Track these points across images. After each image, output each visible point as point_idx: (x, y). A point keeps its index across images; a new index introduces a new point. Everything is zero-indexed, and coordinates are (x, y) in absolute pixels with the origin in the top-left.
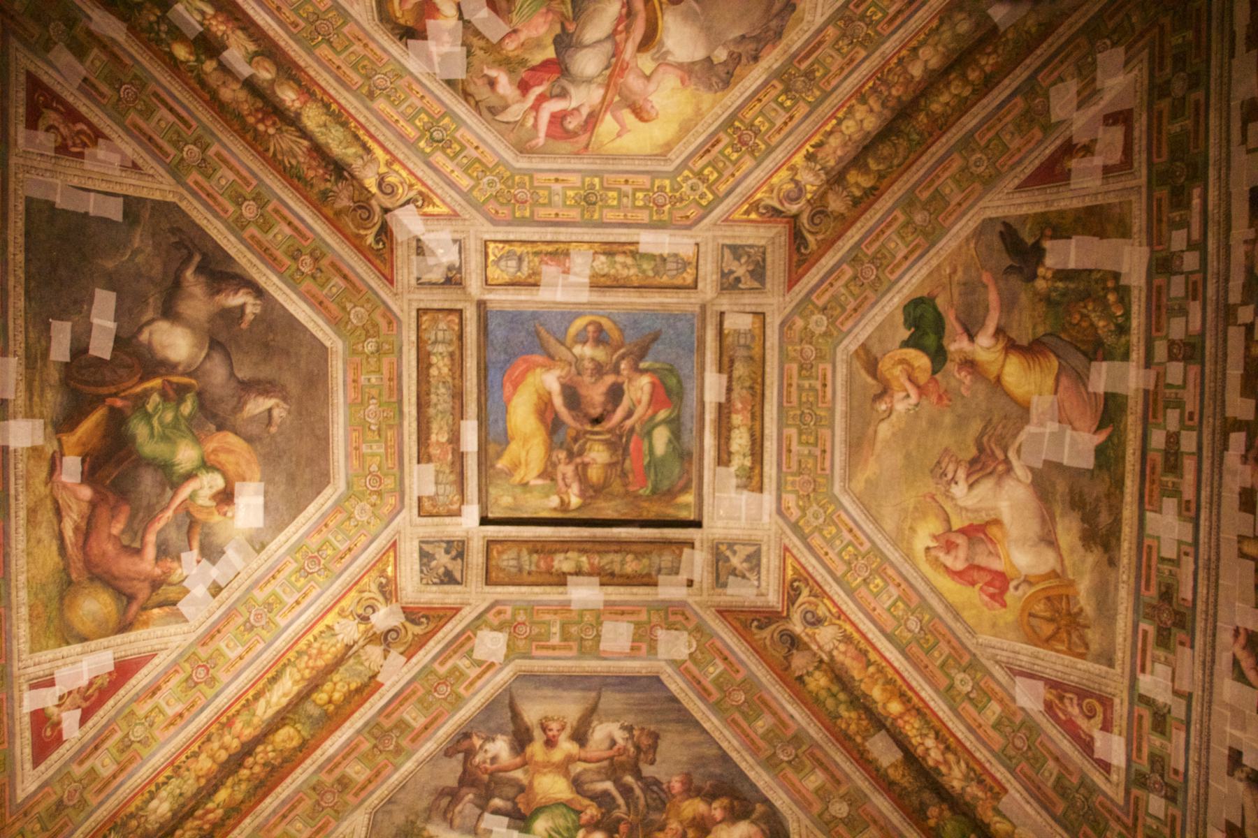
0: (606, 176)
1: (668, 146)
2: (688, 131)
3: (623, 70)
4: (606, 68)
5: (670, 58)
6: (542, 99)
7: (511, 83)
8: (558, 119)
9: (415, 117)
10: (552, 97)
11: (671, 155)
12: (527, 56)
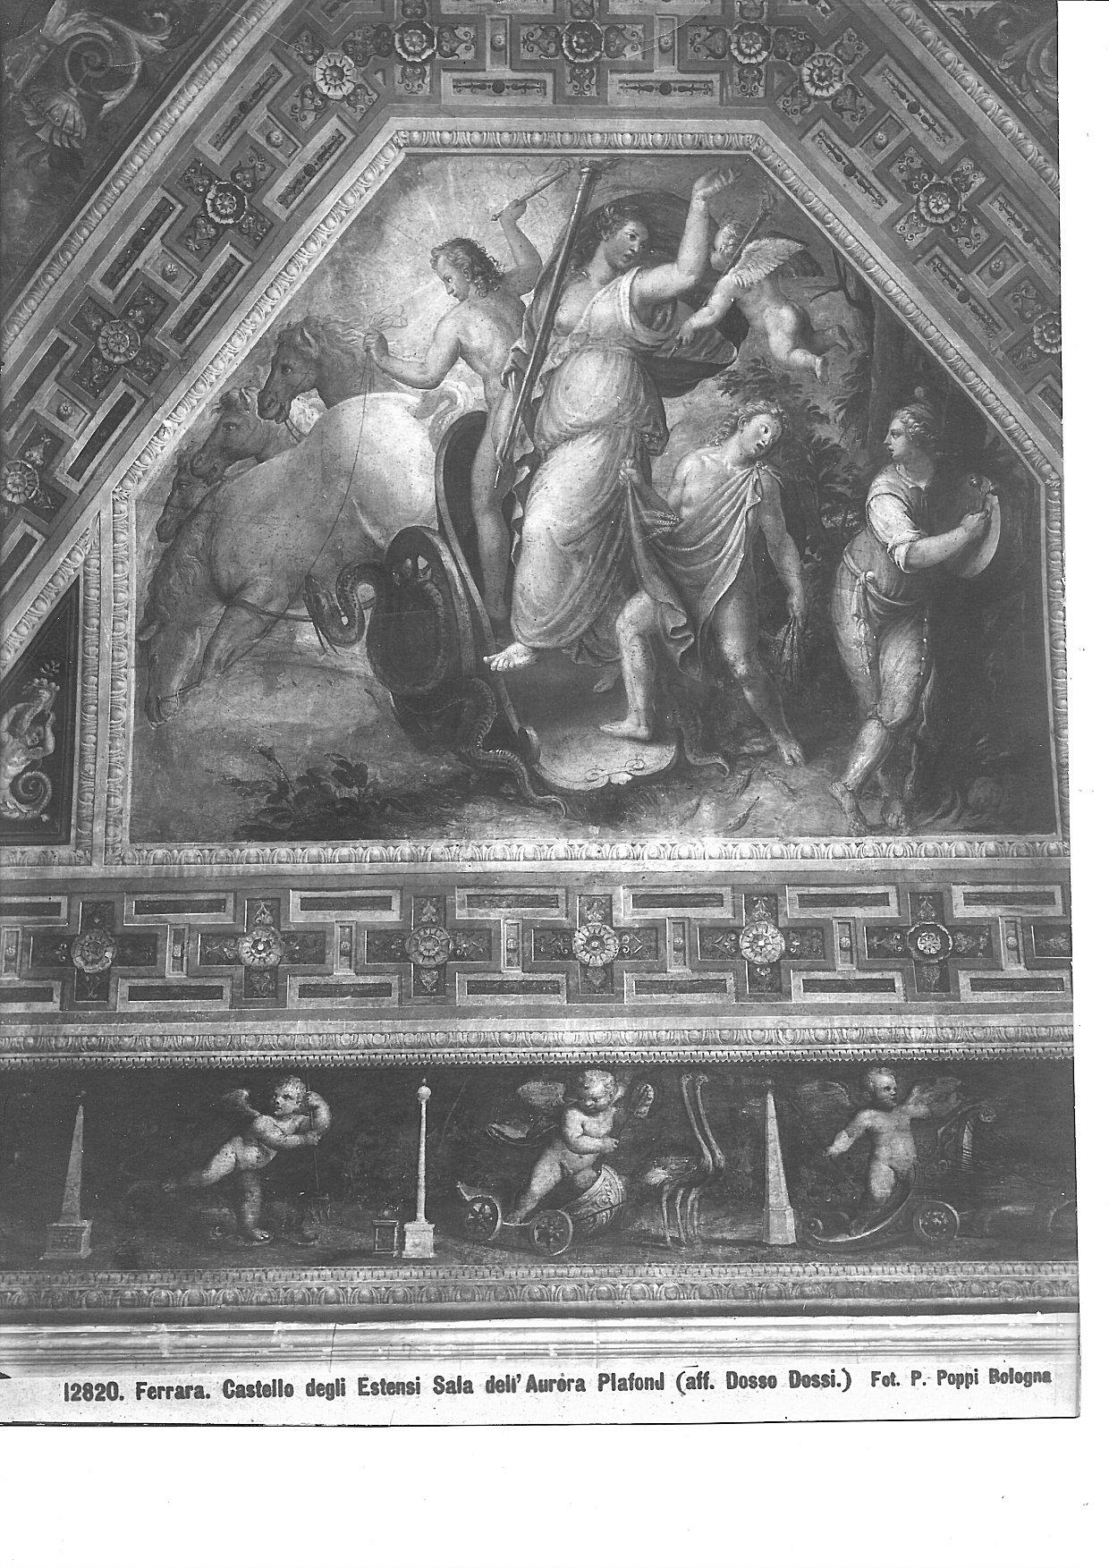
0: (548, 102)
1: (404, 182)
2: (362, 220)
3: (517, 370)
4: (552, 371)
5: (413, 398)
6: (695, 296)
7: (766, 335)
8: (660, 248)
9: (987, 248)
10: (673, 300)
11: (396, 158)
12: (726, 400)
